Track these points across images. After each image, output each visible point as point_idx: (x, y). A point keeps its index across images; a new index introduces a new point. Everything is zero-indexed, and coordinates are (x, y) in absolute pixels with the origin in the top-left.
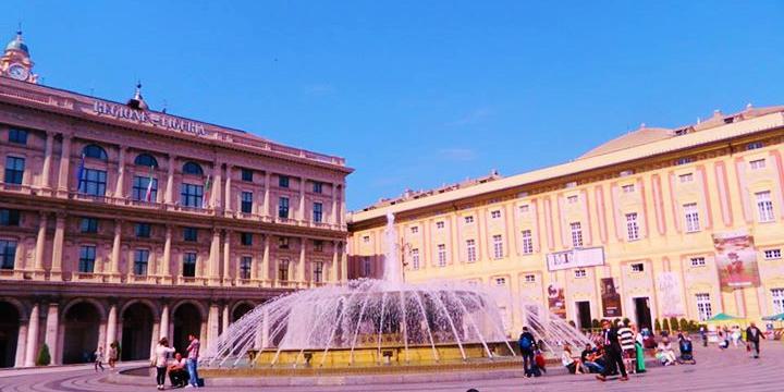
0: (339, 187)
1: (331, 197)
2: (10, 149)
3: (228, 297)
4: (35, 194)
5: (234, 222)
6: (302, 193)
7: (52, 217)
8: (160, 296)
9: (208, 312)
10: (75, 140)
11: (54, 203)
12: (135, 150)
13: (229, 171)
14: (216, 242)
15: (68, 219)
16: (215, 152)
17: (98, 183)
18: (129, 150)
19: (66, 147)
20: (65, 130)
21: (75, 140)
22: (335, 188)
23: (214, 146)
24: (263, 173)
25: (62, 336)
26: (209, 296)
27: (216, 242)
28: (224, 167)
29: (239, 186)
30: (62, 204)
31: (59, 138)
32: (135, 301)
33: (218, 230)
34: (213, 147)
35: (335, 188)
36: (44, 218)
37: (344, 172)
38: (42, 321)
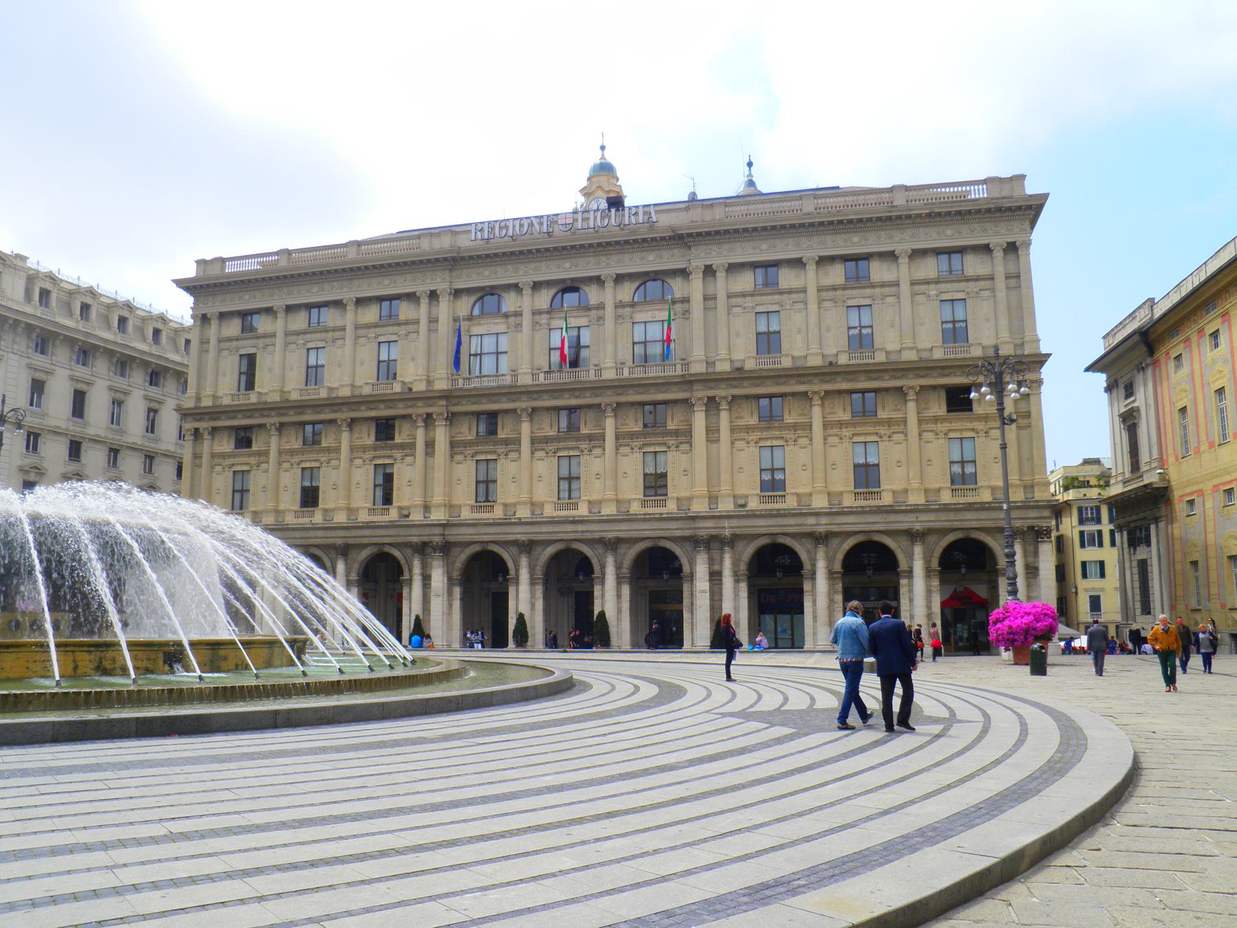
0: (1012, 248)
1: (991, 278)
2: (380, 330)
3: (727, 533)
4: (410, 389)
5: (739, 375)
6: (905, 287)
7: (429, 419)
8: (597, 535)
9: (692, 563)
10: (457, 293)
11: (429, 397)
12: (549, 284)
13: (721, 275)
14: (699, 420)
15: (452, 418)
16: (690, 248)
17: (498, 353)
18: (537, 286)
19: (444, 309)
20: (440, 282)
21: (457, 293)
22: (998, 254)
23: (681, 237)
24: (798, 263)
25: (457, 604)
26: (687, 533)
27: (699, 420)
28: (709, 271)
29: (749, 302)
30: (440, 398)
31: (433, 295)
32: (560, 546)
33: (699, 399)
34: (681, 239)
35: (998, 254)
36: (420, 423)
37: (1031, 209)
38: (426, 579)
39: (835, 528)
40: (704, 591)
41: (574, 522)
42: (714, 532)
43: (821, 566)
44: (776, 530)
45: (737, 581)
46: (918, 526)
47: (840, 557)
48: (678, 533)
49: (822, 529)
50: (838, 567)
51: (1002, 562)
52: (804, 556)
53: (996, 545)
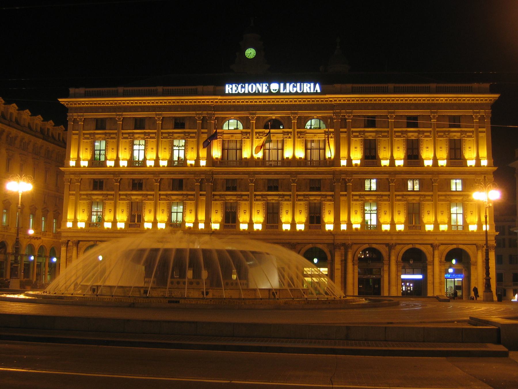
26: (332, 242)
39: (399, 242)
40: (337, 269)
41: (274, 235)
42: (343, 242)
43: (393, 258)
44: (372, 242)
45: (353, 265)
46: (436, 242)
47: (401, 255)
48: (327, 242)
49: (394, 242)
50: (400, 259)
51: (473, 259)
52: (385, 254)
53: (470, 250)
